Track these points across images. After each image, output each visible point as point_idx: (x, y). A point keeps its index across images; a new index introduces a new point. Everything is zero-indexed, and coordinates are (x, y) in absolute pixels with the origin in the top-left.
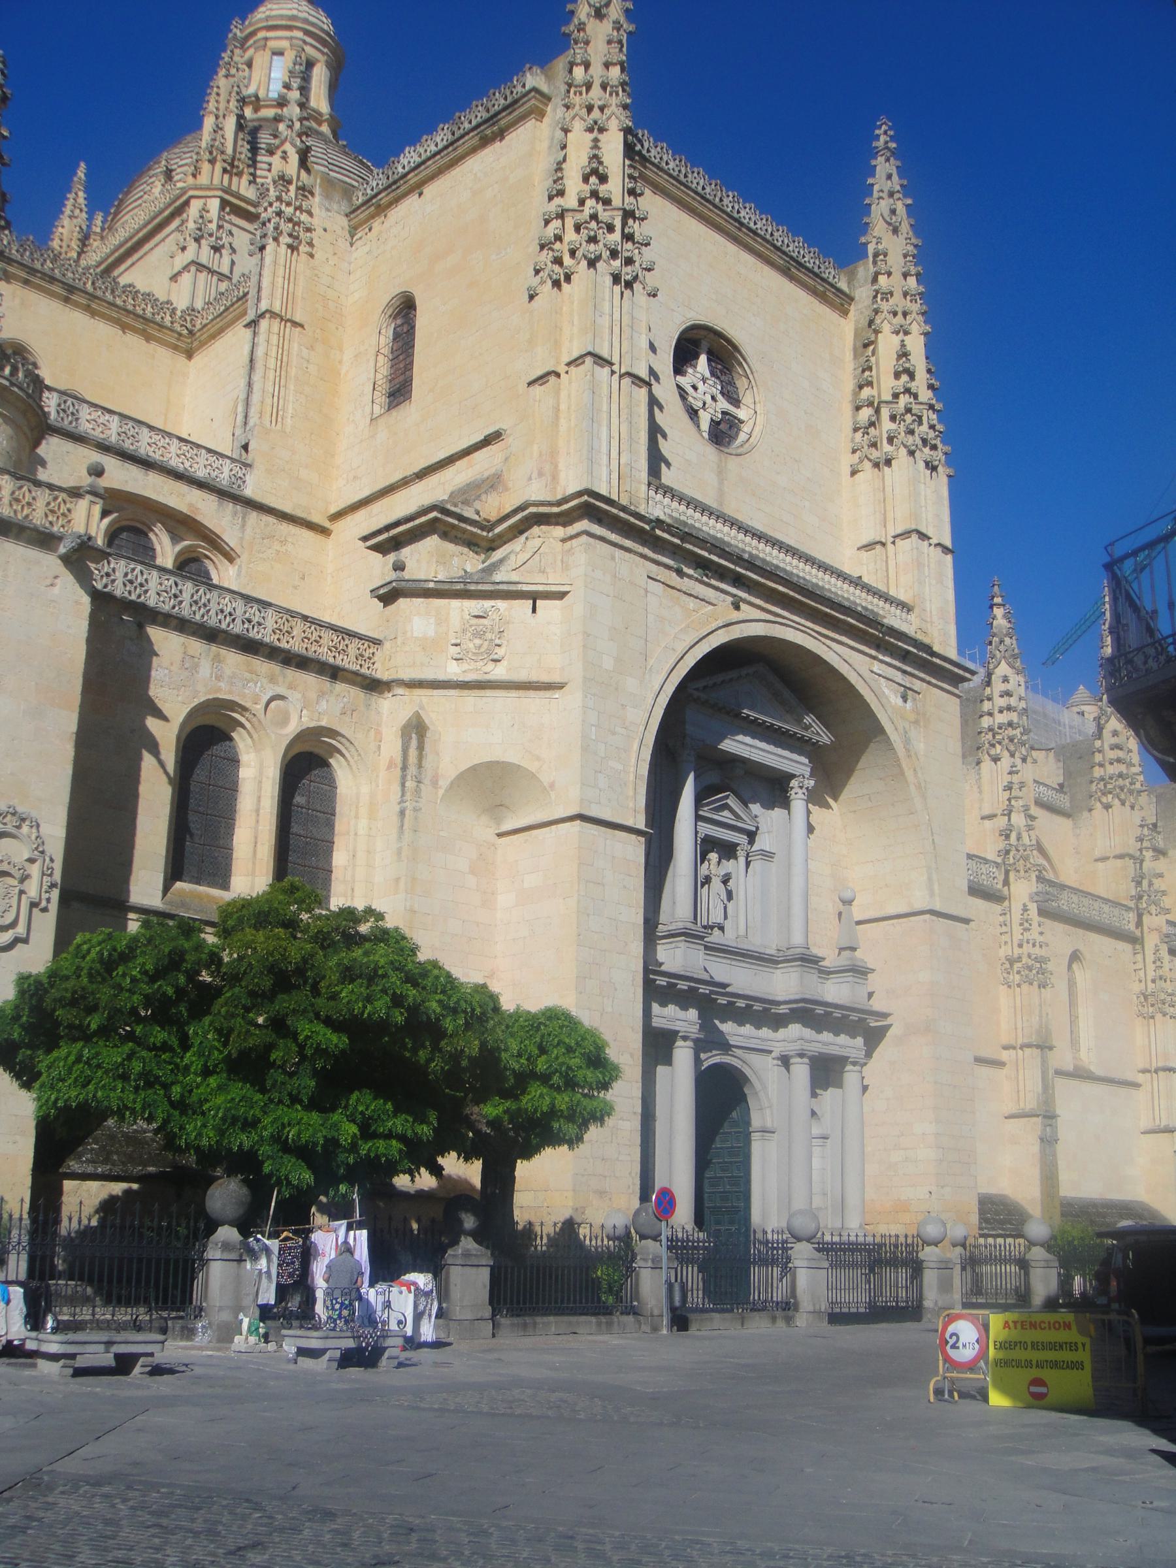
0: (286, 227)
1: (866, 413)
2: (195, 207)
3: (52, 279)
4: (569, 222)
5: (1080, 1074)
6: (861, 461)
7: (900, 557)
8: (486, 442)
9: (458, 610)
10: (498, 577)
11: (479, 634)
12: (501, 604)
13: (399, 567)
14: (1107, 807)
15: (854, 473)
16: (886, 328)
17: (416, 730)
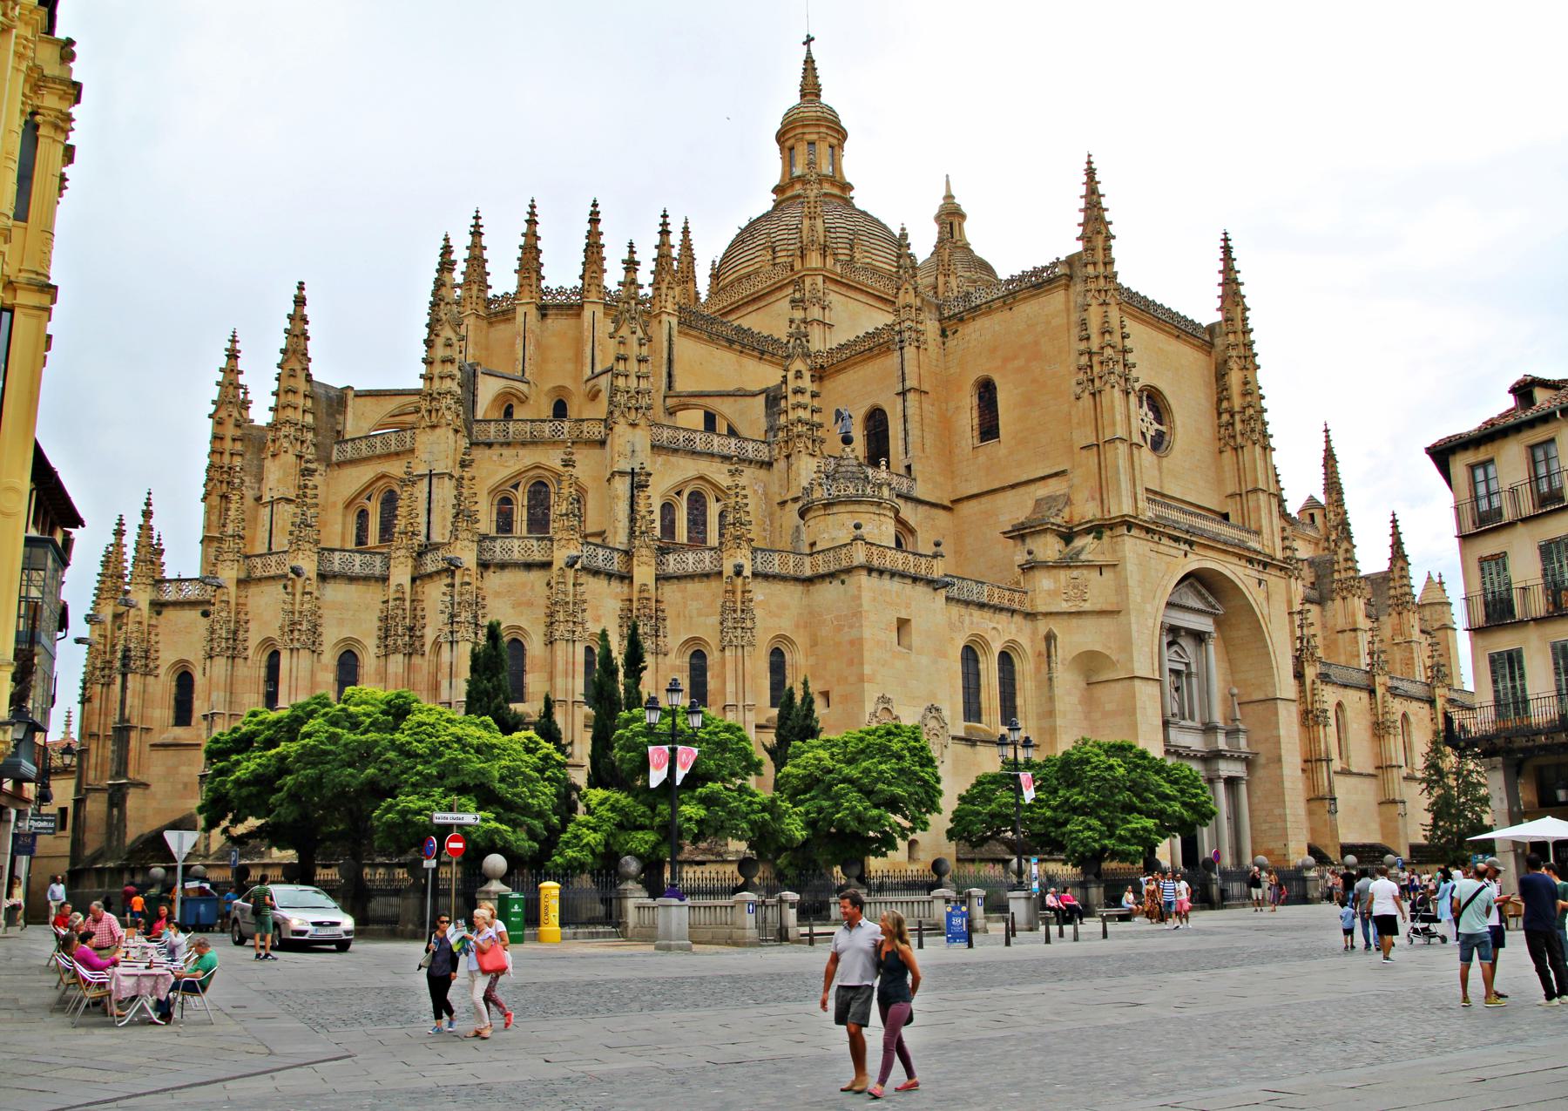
0: (914, 336)
1: (1225, 417)
2: (808, 281)
3: (754, 349)
4: (1095, 359)
5: (1346, 772)
6: (1225, 445)
7: (1251, 504)
8: (1056, 474)
9: (1064, 575)
10: (1083, 557)
11: (1074, 587)
12: (1085, 572)
13: (1030, 553)
14: (1344, 598)
15: (1221, 452)
16: (1235, 367)
17: (1050, 638)
